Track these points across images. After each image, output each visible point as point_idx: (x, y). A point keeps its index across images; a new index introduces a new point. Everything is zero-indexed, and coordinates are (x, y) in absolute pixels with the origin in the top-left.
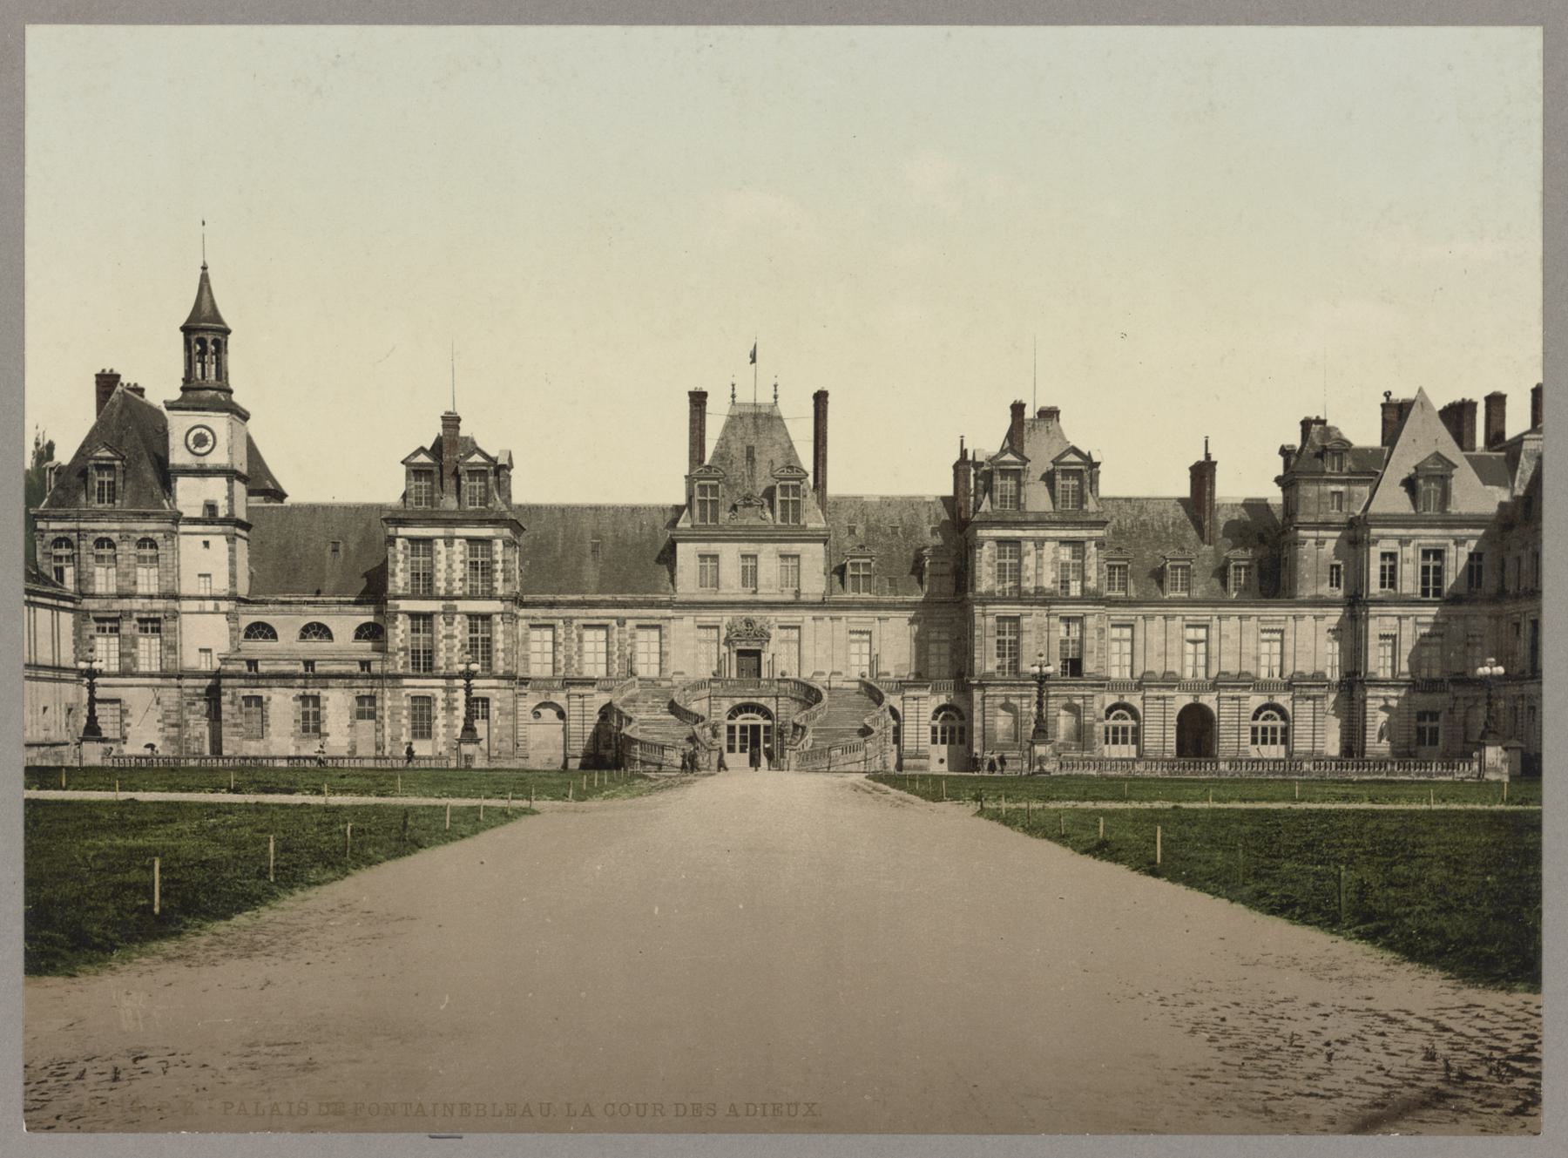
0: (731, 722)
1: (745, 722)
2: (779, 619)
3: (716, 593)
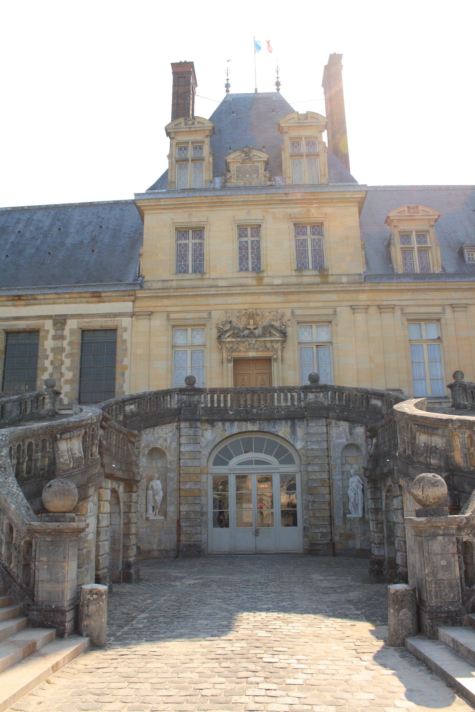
0: (221, 470)
1: (243, 470)
2: (297, 312)
3: (202, 279)
